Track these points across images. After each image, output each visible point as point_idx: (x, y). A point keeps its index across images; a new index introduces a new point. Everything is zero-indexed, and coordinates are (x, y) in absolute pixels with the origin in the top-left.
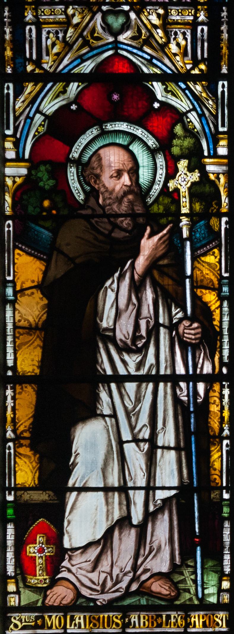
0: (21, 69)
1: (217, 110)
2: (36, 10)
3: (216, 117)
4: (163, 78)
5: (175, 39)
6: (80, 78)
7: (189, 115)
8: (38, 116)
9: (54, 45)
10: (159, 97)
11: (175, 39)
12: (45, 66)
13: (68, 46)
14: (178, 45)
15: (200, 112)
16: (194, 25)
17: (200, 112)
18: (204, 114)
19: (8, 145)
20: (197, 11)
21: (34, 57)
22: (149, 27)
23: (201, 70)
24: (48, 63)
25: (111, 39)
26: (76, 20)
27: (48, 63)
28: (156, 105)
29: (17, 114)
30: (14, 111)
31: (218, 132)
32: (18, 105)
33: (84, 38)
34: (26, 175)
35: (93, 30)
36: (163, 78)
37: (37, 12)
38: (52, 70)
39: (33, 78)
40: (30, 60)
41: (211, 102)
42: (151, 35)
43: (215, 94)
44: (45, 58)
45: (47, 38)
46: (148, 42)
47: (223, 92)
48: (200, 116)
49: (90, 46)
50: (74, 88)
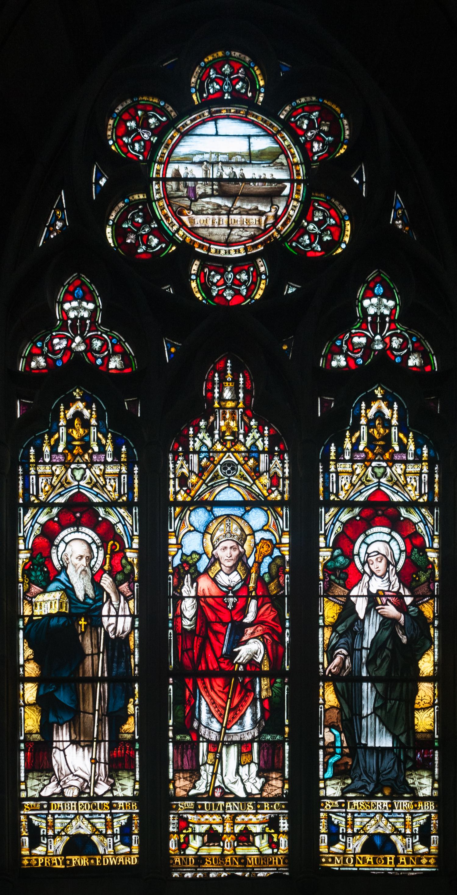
0: (27, 500)
1: (133, 522)
2: (36, 467)
3: (132, 526)
4: (104, 505)
5: (109, 482)
6: (59, 505)
7: (118, 525)
8: (36, 524)
9: (45, 486)
10: (101, 515)
11: (109, 482)
12: (40, 498)
13: (53, 487)
14: (111, 486)
15: (123, 523)
16: (120, 474)
17: (123, 523)
18: (125, 524)
19: (21, 541)
20: (121, 466)
21: (35, 494)
22: (95, 475)
23: (123, 500)
24: (42, 497)
25: (76, 483)
26: (57, 473)
27: (42, 497)
28: (100, 519)
29: (25, 524)
30: (24, 523)
31: (133, 535)
32: (26, 518)
33: (61, 483)
34: (30, 557)
35: (66, 478)
36: (104, 505)
37: (36, 468)
38: (44, 500)
39: (34, 506)
40: (33, 495)
41: (129, 518)
42: (97, 482)
43: (132, 514)
44: (41, 493)
45: (42, 483)
46: (95, 485)
47: (136, 513)
48: (123, 525)
49: (65, 487)
50: (55, 511)
